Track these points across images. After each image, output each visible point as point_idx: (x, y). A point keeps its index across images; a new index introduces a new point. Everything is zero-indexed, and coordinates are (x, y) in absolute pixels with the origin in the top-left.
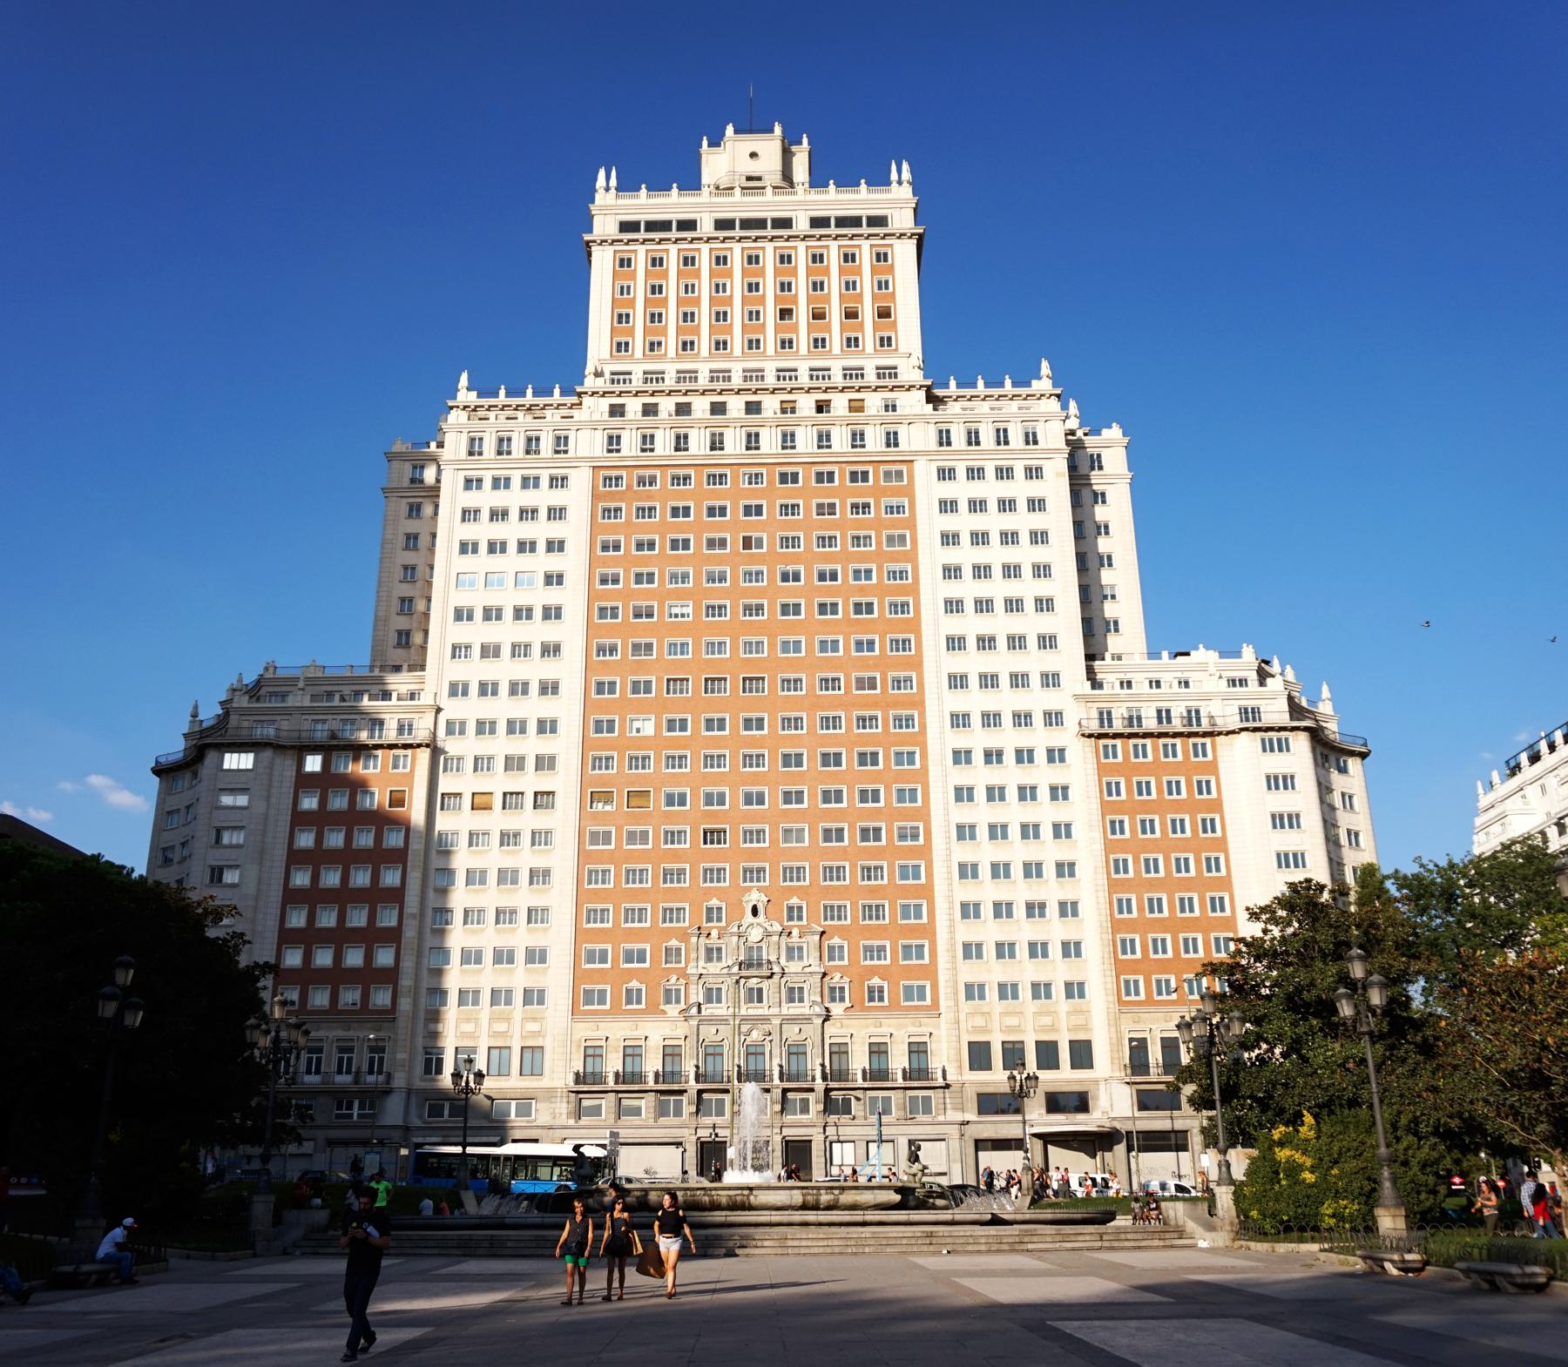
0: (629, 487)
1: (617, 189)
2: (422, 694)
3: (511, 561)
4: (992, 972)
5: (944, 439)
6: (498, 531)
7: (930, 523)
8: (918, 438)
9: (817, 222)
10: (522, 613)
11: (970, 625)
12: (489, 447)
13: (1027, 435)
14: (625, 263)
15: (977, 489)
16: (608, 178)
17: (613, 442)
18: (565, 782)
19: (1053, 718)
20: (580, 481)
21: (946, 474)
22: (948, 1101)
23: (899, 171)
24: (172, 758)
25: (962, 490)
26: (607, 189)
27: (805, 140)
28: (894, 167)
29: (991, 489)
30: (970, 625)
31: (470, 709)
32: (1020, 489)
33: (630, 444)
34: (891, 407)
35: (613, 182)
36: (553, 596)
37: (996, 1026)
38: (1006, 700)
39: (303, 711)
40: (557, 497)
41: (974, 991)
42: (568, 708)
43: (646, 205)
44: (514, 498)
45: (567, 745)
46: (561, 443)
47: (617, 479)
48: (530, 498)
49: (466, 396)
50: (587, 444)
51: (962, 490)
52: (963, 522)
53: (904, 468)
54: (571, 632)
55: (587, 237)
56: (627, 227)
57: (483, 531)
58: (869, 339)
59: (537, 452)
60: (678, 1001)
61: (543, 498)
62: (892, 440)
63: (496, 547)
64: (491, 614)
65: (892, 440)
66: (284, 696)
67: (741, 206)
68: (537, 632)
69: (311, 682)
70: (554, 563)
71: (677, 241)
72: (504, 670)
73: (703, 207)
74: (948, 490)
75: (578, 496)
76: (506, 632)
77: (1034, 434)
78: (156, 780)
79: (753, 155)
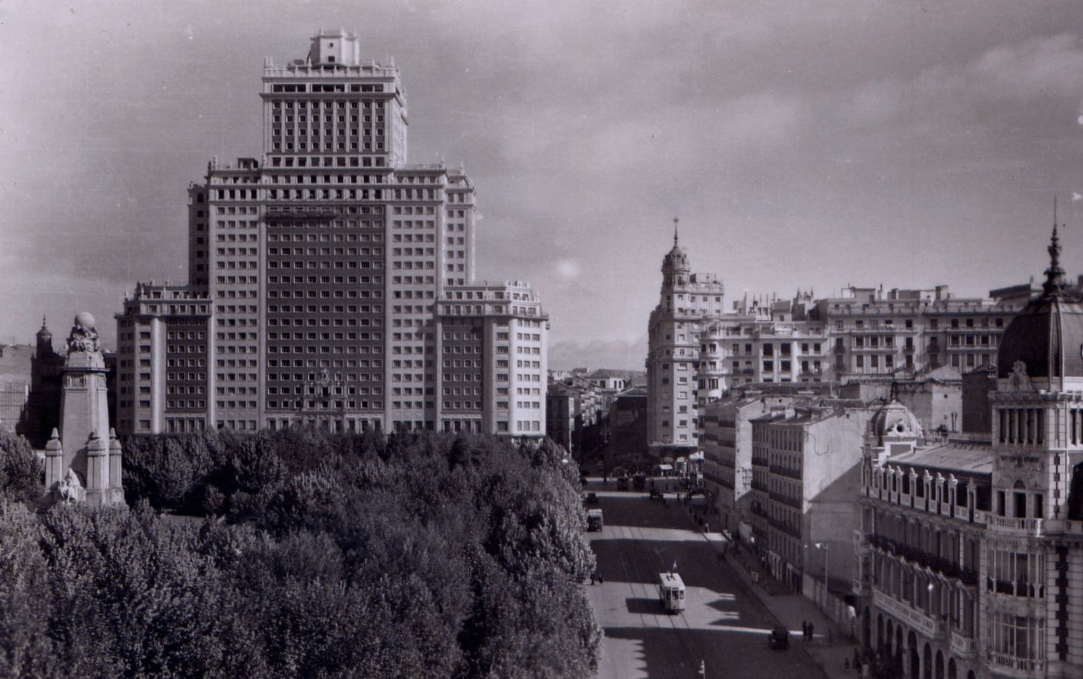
5: (398, 196)
9: (355, 88)
11: (404, 273)
19: (432, 309)
29: (414, 217)
32: (425, 217)
34: (379, 180)
51: (403, 217)
56: (278, 88)
62: (378, 195)
65: (378, 195)
78: (116, 320)
79: (332, 45)
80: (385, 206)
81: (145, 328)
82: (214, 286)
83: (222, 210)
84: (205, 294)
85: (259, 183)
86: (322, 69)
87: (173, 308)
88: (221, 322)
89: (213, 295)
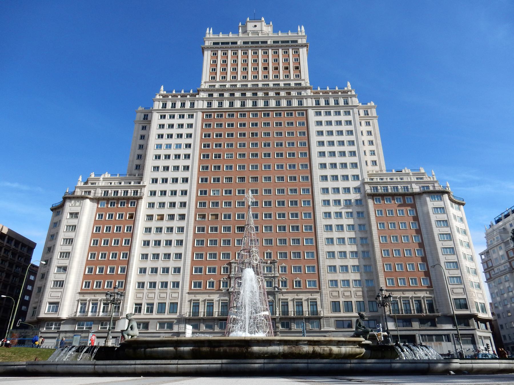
1: (214, 33)
2: (142, 183)
3: (174, 141)
4: (340, 277)
5: (318, 103)
6: (170, 131)
7: (313, 129)
8: (309, 102)
10: (178, 157)
11: (328, 160)
13: (344, 102)
15: (328, 118)
16: (210, 30)
17: (210, 104)
18: (191, 211)
19: (357, 190)
21: (319, 114)
22: (325, 323)
23: (301, 28)
24: (57, 205)
26: (209, 33)
27: (271, 24)
28: (299, 27)
29: (333, 118)
30: (328, 160)
31: (159, 187)
32: (343, 118)
33: (215, 104)
35: (211, 31)
36: (188, 151)
37: (341, 295)
38: (341, 184)
39: (101, 187)
40: (191, 121)
41: (334, 283)
42: (193, 188)
43: (222, 37)
44: (176, 121)
45: (192, 199)
46: (192, 105)
48: (181, 121)
49: (162, 92)
50: (201, 105)
51: (323, 118)
54: (195, 163)
55: (203, 46)
60: (226, 286)
61: (186, 121)
62: (300, 103)
63: (170, 136)
64: (168, 157)
65: (300, 103)
66: (95, 183)
67: (251, 37)
68: (182, 162)
71: (231, 48)
72: (170, 175)
73: (240, 38)
74: (319, 118)
76: (171, 163)
77: (347, 101)
79: (255, 26)
80: (306, 111)
81: (75, 210)
82: (148, 174)
83: (163, 117)
84: (141, 177)
85: (197, 96)
87: (106, 193)
88: (151, 205)
89: (147, 181)
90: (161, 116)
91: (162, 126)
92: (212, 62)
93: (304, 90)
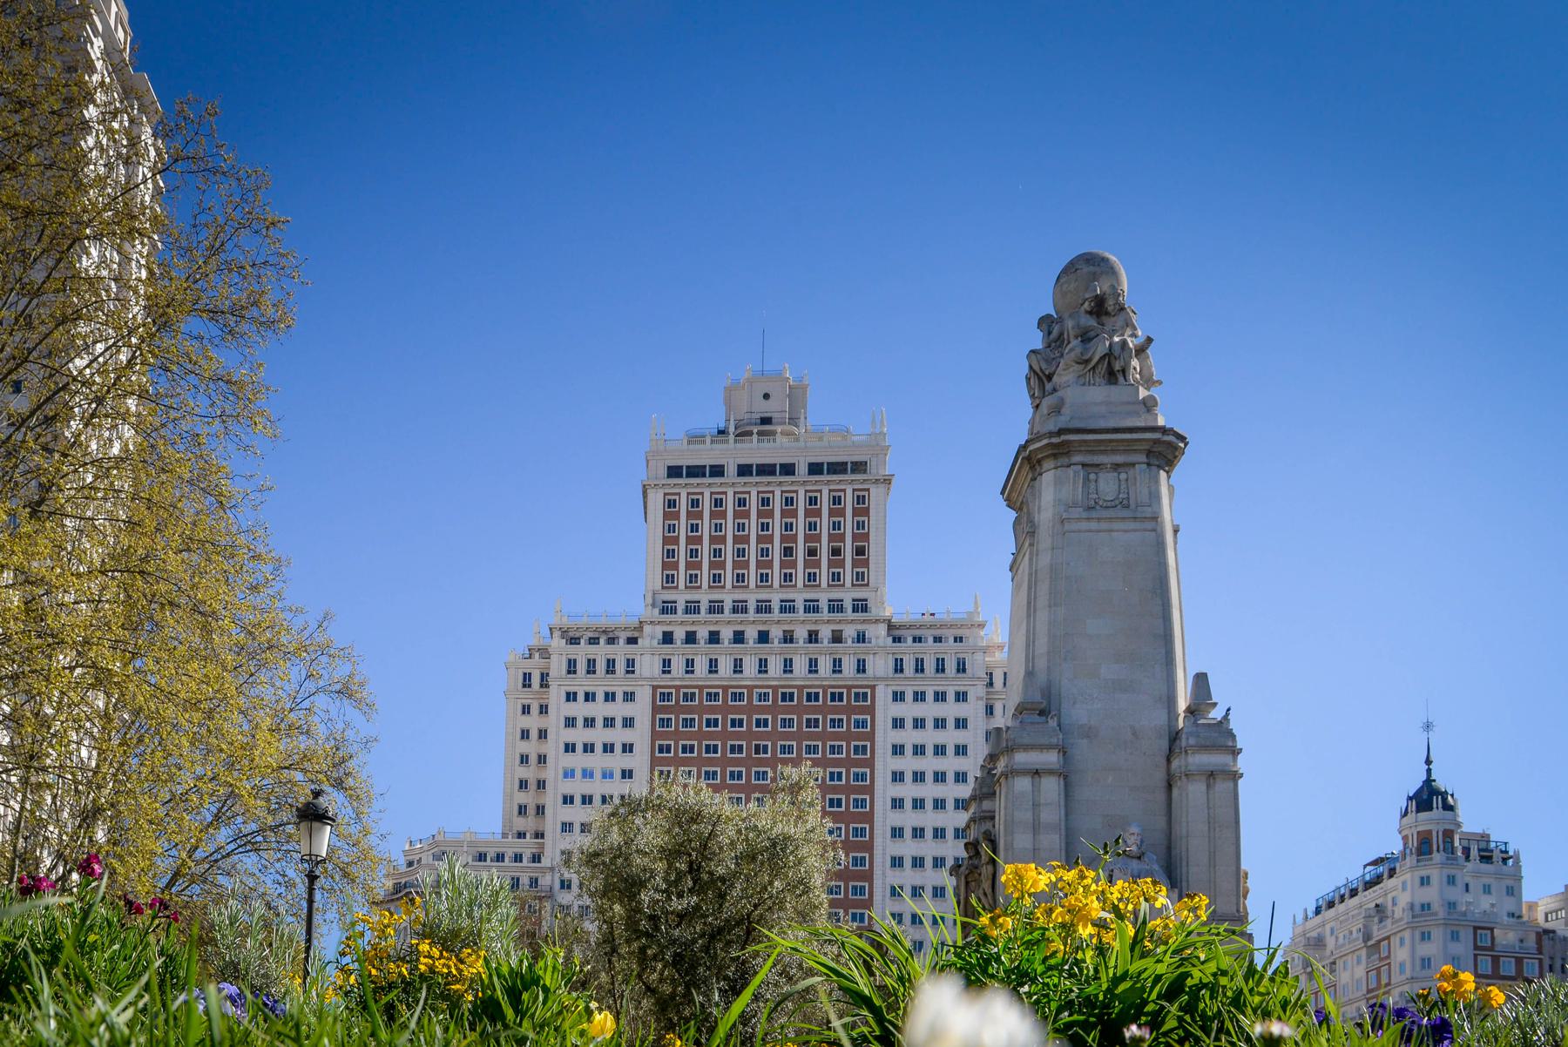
0: (677, 701)
3: (598, 761)
9: (815, 469)
12: (581, 667)
14: (672, 504)
17: (667, 663)
20: (644, 696)
21: (898, 697)
25: (909, 710)
29: (929, 710)
33: (678, 666)
34: (861, 638)
46: (630, 663)
47: (668, 694)
51: (909, 710)
52: (909, 737)
53: (869, 691)
56: (674, 472)
57: (579, 735)
58: (848, 577)
59: (613, 672)
61: (618, 710)
62: (861, 667)
63: (589, 748)
65: (861, 667)
69: (471, 844)
70: (626, 761)
74: (899, 710)
75: (641, 709)
77: (964, 664)
80: (873, 688)
86: (755, 437)
90: (568, 694)
91: (570, 722)
92: (666, 528)
93: (873, 625)
